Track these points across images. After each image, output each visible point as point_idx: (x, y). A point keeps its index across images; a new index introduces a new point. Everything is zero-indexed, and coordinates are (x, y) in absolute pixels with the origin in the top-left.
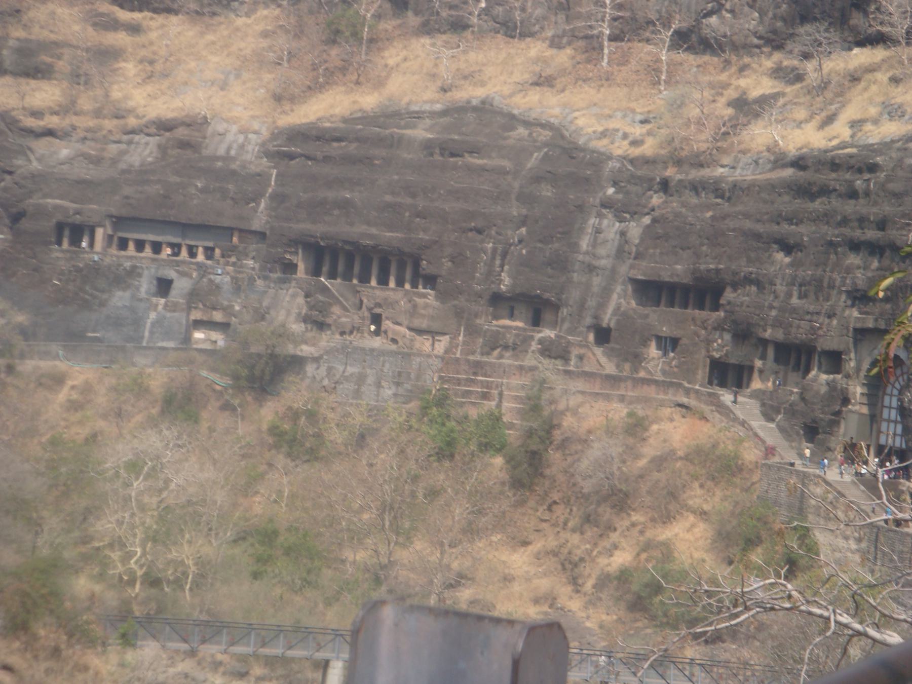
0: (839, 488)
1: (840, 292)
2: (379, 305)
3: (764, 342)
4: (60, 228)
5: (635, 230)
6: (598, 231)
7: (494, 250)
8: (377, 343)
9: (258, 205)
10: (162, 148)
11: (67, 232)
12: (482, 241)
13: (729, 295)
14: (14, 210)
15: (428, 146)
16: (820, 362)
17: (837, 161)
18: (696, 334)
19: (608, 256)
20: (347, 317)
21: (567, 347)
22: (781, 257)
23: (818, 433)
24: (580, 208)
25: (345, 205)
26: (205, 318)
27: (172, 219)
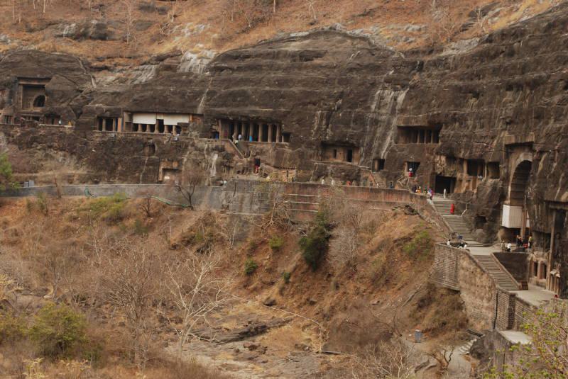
0: (477, 261)
1: (499, 120)
2: (257, 154)
3: (462, 160)
4: (100, 119)
5: (402, 96)
6: (381, 98)
7: (322, 114)
8: (255, 177)
9: (201, 99)
10: (157, 71)
11: (104, 123)
12: (316, 110)
13: (443, 132)
14: (79, 112)
15: (293, 56)
16: (487, 170)
17: (505, 33)
18: (428, 158)
19: (387, 113)
20: (242, 162)
21: (359, 173)
22: (473, 101)
23: (486, 221)
24: (374, 85)
25: (244, 94)
26: (169, 167)
27: (158, 111)
